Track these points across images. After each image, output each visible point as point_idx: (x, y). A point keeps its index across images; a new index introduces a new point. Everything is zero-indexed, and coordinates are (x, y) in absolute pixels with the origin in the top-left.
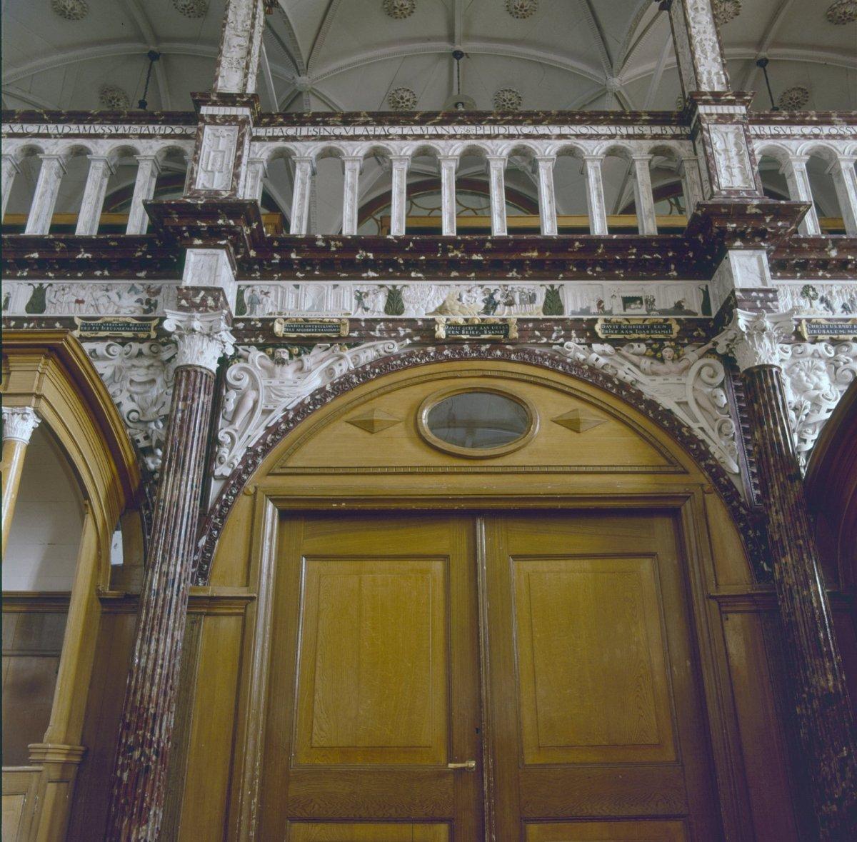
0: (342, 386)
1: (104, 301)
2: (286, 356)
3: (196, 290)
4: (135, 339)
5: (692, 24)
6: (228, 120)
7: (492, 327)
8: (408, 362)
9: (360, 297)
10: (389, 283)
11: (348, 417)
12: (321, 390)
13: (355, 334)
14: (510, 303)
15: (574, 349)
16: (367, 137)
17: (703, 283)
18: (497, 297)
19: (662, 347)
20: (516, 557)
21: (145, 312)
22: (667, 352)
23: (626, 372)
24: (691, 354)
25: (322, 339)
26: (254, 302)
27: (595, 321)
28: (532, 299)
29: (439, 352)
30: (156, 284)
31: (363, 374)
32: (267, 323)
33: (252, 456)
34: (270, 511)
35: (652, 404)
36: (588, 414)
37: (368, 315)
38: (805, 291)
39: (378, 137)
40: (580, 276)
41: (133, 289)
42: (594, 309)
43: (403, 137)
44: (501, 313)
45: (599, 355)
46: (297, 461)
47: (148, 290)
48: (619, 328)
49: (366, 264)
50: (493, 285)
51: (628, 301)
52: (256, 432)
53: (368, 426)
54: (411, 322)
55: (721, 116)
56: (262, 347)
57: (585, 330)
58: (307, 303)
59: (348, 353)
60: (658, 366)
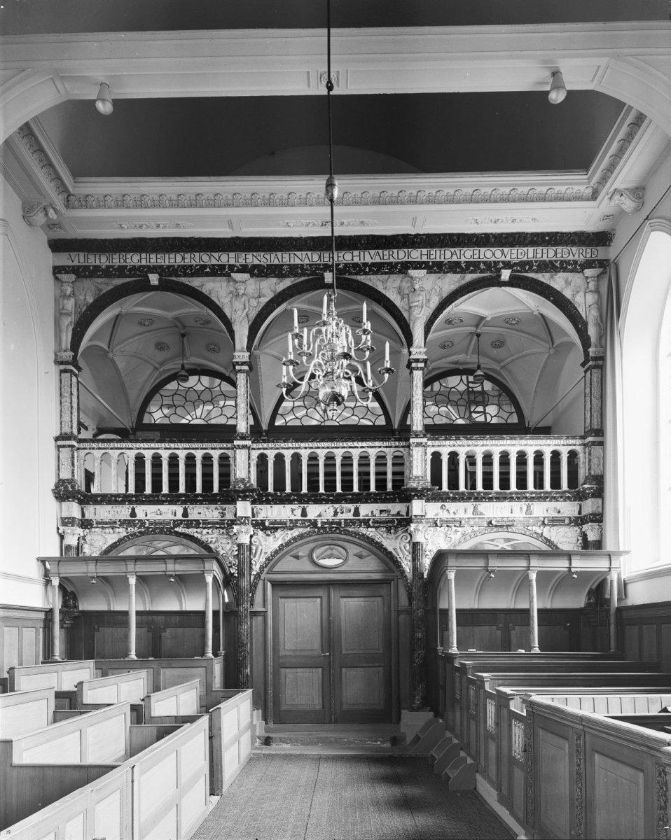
0: (288, 544)
1: (207, 513)
2: (269, 533)
3: (242, 517)
4: (221, 528)
5: (414, 395)
6: (244, 447)
7: (336, 523)
8: (309, 534)
9: (293, 510)
10: (302, 505)
11: (291, 554)
12: (282, 545)
13: (291, 525)
14: (342, 513)
15: (363, 530)
16: (293, 448)
17: (407, 504)
18: (338, 510)
19: (391, 529)
20: (342, 597)
21: (222, 517)
22: (392, 531)
23: (378, 538)
24: (400, 530)
25: (281, 527)
26: (258, 513)
27: (370, 520)
28: (350, 511)
29: (319, 531)
30: (224, 506)
31: (295, 539)
32: (263, 522)
33: (262, 568)
34: (269, 585)
35: (386, 549)
36: (365, 553)
37: (296, 518)
38: (442, 507)
39: (297, 448)
40: (366, 502)
41: (216, 508)
42: (370, 515)
43: (306, 448)
44: (340, 516)
45: (371, 532)
46: (276, 569)
47: (222, 508)
48: (378, 522)
49: (294, 500)
50: (336, 506)
51: (381, 511)
52: (263, 560)
53: (297, 557)
54: (310, 520)
55: (418, 443)
56: (262, 530)
57: (366, 523)
58: (275, 513)
59: (290, 532)
60: (390, 536)
